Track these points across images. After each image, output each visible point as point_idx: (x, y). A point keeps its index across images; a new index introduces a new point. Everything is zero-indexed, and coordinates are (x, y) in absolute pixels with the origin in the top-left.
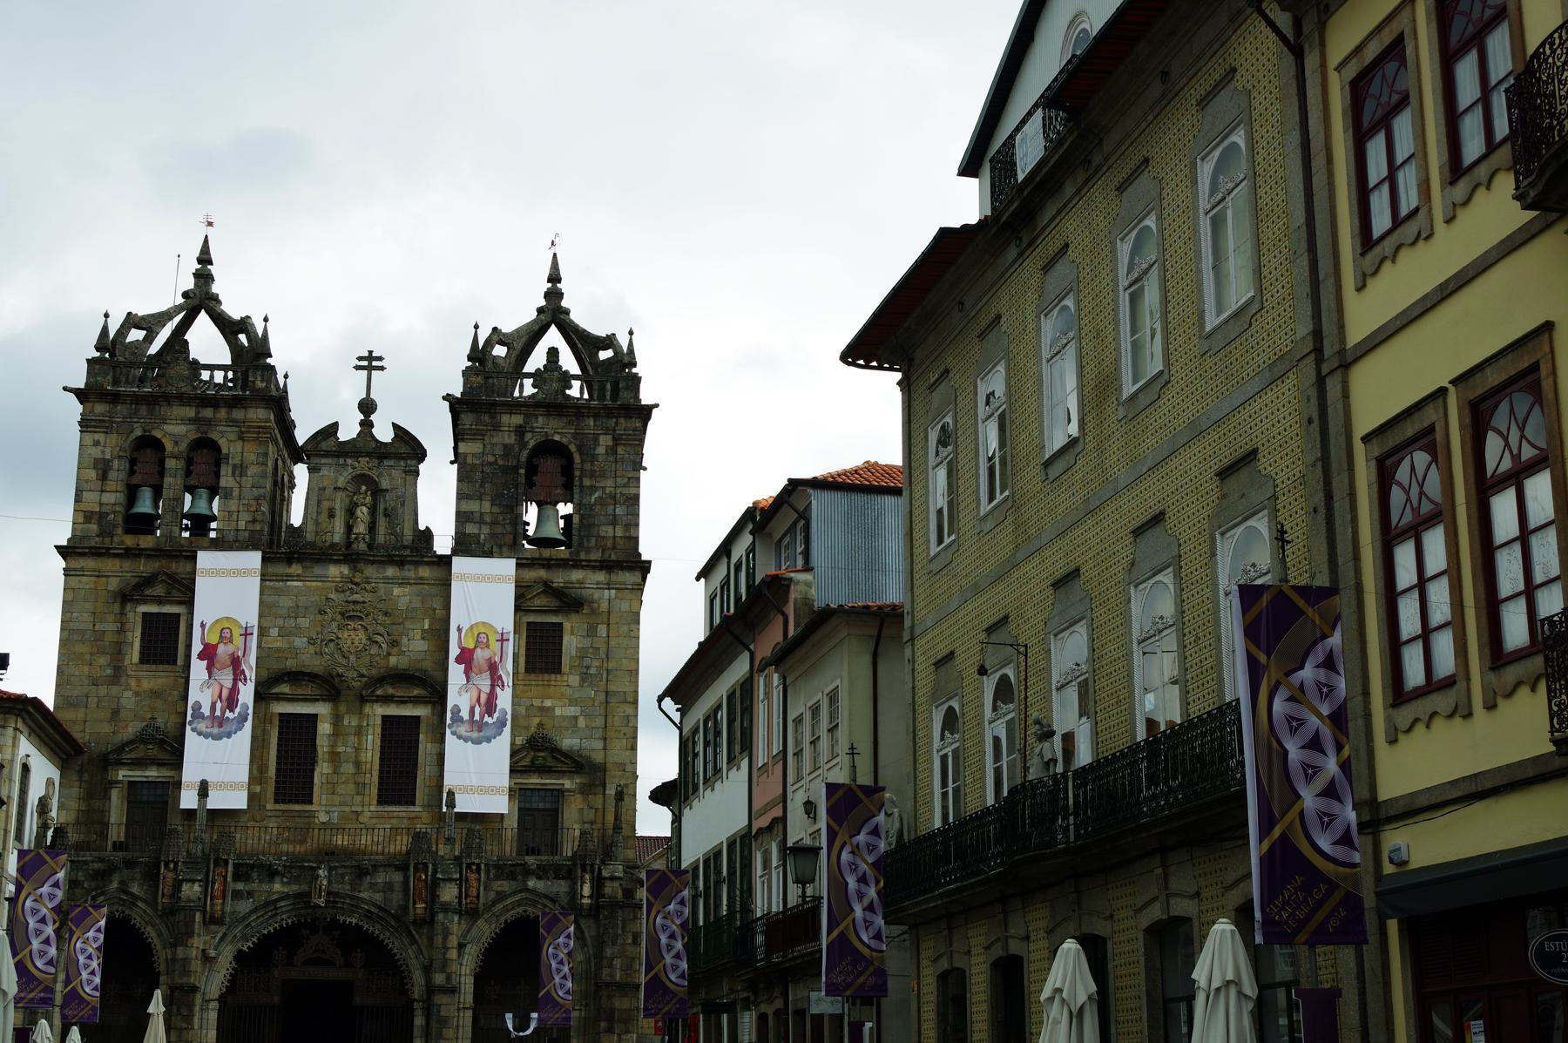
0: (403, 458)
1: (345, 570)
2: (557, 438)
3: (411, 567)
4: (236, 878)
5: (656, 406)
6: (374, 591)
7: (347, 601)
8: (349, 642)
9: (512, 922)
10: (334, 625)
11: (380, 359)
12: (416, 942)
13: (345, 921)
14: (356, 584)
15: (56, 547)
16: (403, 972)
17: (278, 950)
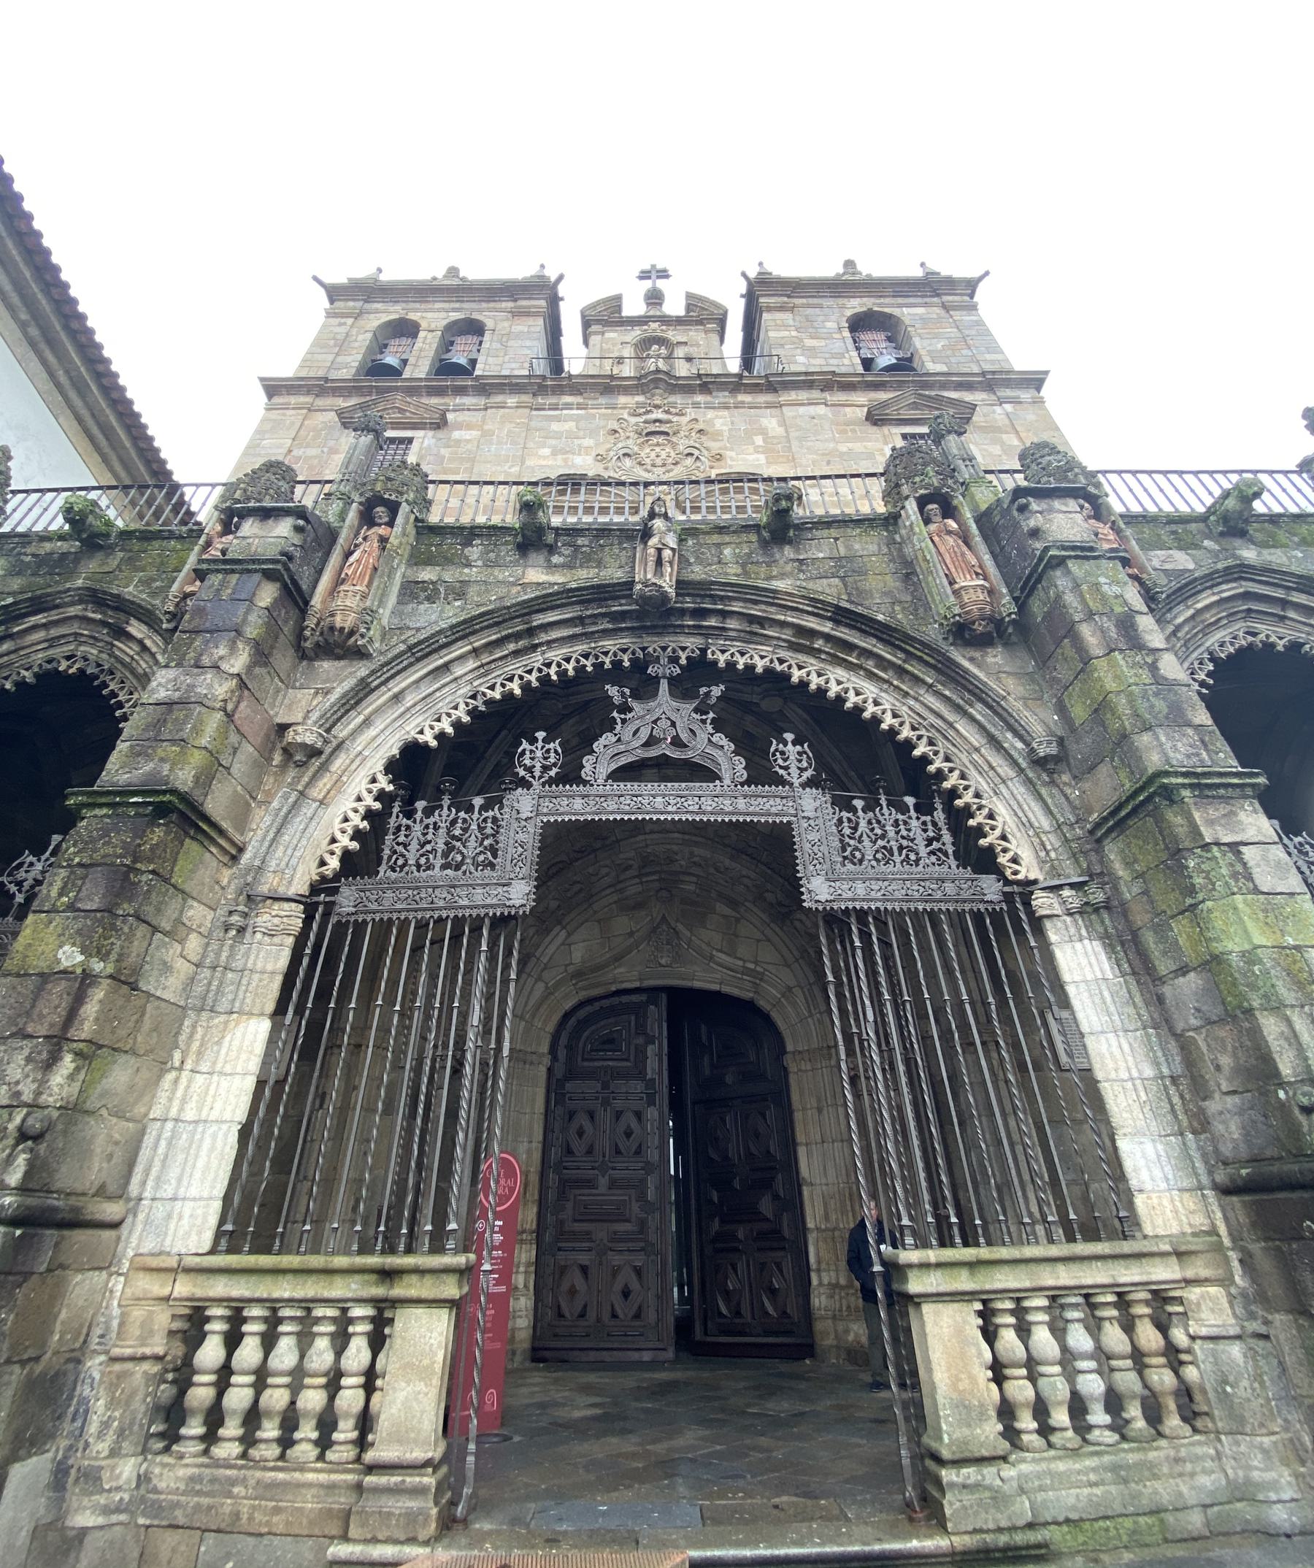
0: (700, 322)
1: (640, 398)
2: (876, 309)
3: (727, 394)
4: (419, 558)
5: (987, 273)
6: (681, 414)
7: (645, 422)
8: (653, 455)
9: (1230, 656)
10: (630, 442)
11: (665, 271)
12: (978, 693)
13: (731, 665)
14: (657, 407)
15: (262, 379)
16: (953, 794)
17: (533, 741)
